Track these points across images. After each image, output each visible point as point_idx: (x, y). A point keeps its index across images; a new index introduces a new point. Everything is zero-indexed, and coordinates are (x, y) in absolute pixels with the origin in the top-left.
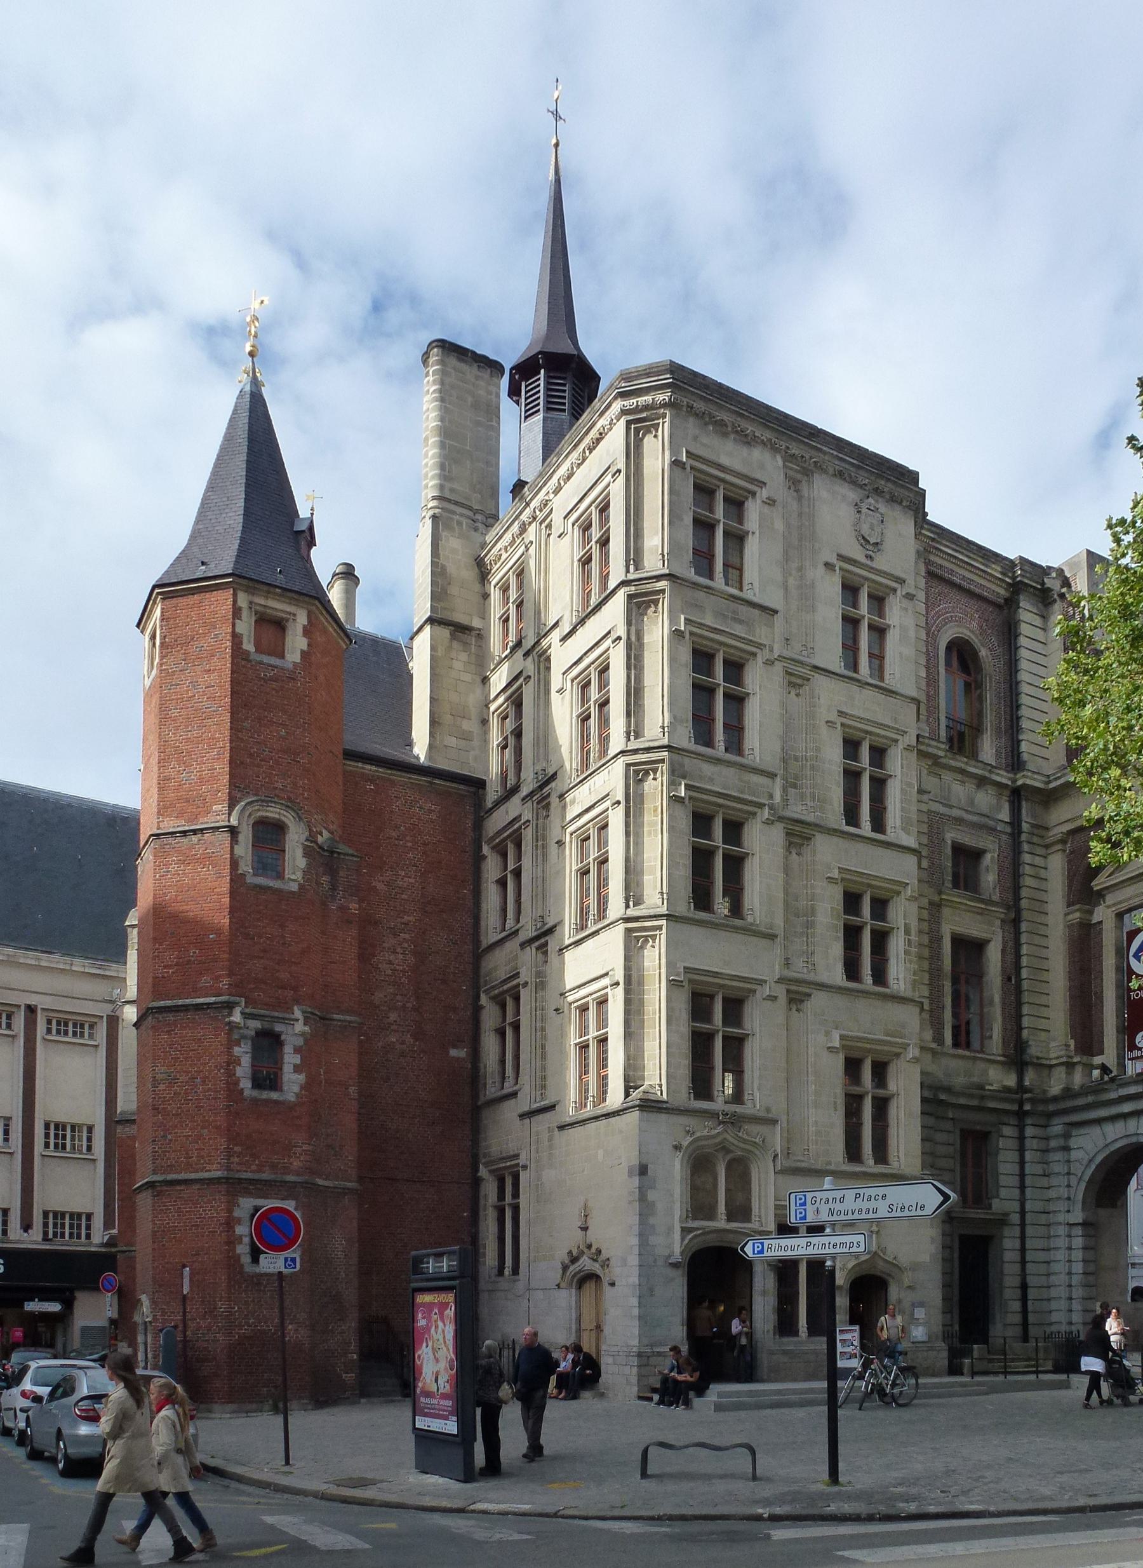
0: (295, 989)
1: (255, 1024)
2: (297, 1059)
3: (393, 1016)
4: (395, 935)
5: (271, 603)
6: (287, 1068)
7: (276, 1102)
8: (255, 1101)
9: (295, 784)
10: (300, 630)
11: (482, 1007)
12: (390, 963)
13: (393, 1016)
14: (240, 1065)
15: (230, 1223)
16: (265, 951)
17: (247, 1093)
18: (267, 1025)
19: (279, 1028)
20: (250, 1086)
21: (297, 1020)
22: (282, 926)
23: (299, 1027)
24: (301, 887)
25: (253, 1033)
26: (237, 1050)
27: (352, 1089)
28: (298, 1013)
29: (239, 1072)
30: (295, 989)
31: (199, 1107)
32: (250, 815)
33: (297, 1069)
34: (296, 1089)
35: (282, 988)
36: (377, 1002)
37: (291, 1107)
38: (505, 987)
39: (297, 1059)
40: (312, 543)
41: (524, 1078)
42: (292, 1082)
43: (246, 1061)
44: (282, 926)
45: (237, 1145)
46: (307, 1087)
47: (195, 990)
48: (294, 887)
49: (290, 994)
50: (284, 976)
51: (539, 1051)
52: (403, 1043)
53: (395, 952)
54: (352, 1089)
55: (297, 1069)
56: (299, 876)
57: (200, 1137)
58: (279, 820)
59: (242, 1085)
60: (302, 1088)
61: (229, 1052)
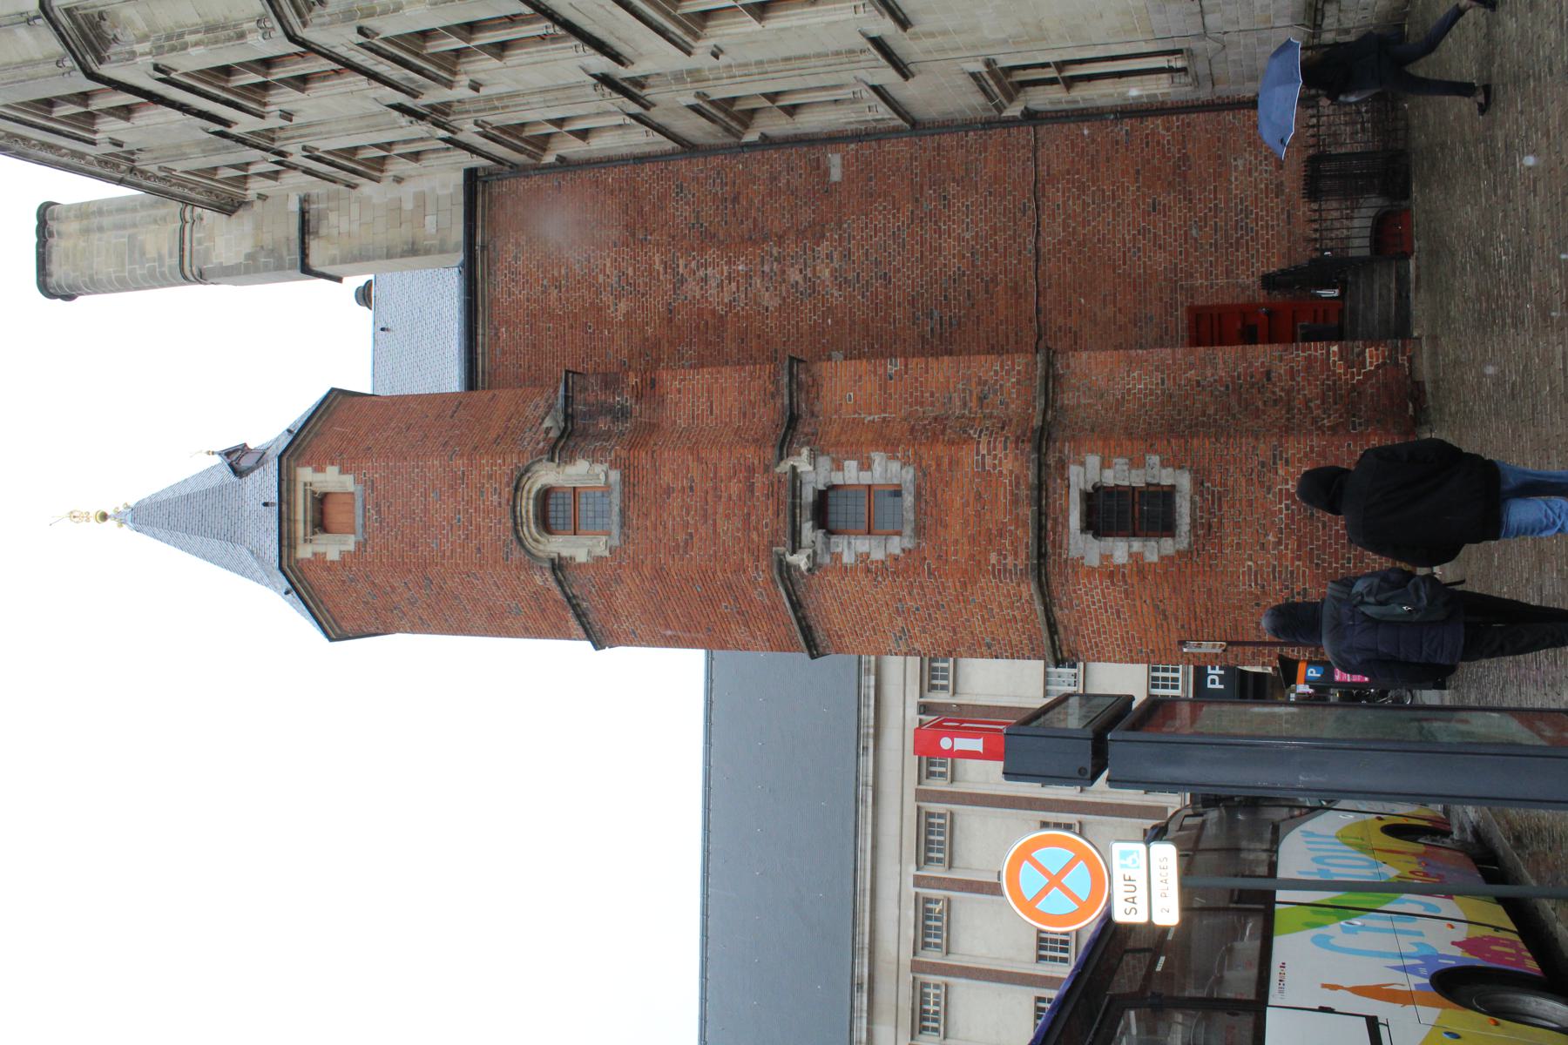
0: (751, 470)
1: (807, 528)
2: (851, 466)
3: (794, 276)
4: (682, 281)
5: (300, 516)
6: (865, 478)
7: (918, 496)
8: (919, 531)
9: (490, 477)
10: (319, 477)
11: (764, 137)
12: (720, 285)
13: (794, 276)
14: (868, 555)
15: (1112, 573)
16: (705, 517)
17: (908, 543)
18: (807, 513)
19: (808, 496)
20: (896, 539)
21: (794, 468)
22: (668, 491)
23: (802, 462)
24: (613, 465)
25: (820, 533)
26: (848, 559)
27: (891, 369)
28: (785, 467)
29: (878, 555)
30: (751, 470)
31: (938, 606)
32: (536, 541)
33: (866, 465)
34: (895, 466)
35: (752, 492)
36: (777, 302)
37: (922, 472)
38: (721, 115)
39: (851, 466)
40: (243, 449)
41: (846, 77)
42: (885, 470)
43: (862, 545)
44: (668, 491)
45: (987, 561)
46: (890, 446)
47: (775, 607)
48: (615, 476)
49: (759, 480)
50: (735, 488)
51: (797, 64)
52: (829, 256)
53: (705, 280)
54: (891, 369)
55: (866, 465)
56: (599, 469)
57: (983, 606)
58: (536, 499)
59: (897, 551)
60: (894, 458)
61: (854, 569)
